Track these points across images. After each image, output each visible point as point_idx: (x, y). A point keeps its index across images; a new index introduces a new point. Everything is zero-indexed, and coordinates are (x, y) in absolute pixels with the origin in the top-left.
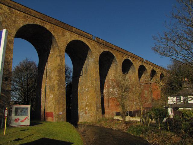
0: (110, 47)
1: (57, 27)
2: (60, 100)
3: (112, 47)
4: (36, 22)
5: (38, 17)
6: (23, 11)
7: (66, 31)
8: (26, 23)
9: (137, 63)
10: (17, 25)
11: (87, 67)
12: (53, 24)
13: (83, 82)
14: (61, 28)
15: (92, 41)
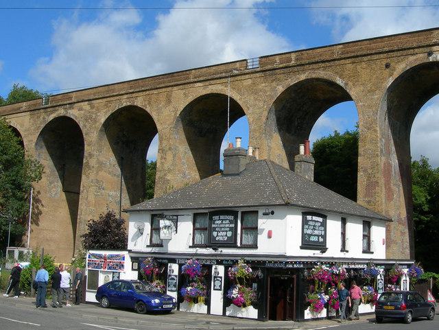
1: (155, 92)
7: (175, 88)
12: (148, 90)
14: (164, 90)
15: (243, 77)
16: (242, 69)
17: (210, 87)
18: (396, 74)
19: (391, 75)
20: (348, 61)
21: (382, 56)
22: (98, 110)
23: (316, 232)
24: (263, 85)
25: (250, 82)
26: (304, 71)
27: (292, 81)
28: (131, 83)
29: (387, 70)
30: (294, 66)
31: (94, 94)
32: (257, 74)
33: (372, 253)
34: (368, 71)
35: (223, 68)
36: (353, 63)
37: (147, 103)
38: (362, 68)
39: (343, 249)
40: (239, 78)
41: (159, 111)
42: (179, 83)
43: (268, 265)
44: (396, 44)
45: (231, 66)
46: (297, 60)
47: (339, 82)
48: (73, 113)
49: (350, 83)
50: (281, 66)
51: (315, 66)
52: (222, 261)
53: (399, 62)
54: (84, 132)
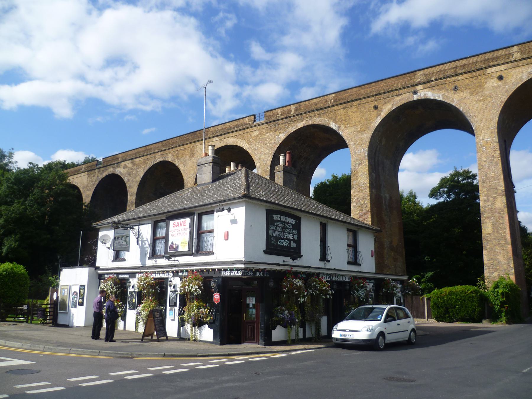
0: (313, 111)
1: (182, 148)
3: (319, 106)
7: (197, 144)
12: (176, 147)
14: (188, 145)
15: (251, 129)
16: (251, 122)
17: (225, 140)
18: (383, 114)
19: (379, 115)
20: (339, 107)
21: (370, 99)
22: (138, 166)
23: (286, 235)
24: (268, 134)
25: (257, 133)
26: (302, 120)
27: (292, 129)
28: (164, 143)
29: (376, 111)
30: (293, 116)
32: (263, 126)
33: (360, 265)
34: (358, 114)
35: (235, 123)
36: (345, 108)
37: (175, 157)
38: (353, 112)
39: (324, 257)
40: (248, 130)
41: (185, 163)
43: (224, 274)
44: (382, 86)
46: (296, 110)
47: (333, 126)
48: (120, 171)
49: (342, 126)
50: (283, 117)
51: (311, 114)
52: (177, 272)
53: (386, 103)
54: (128, 185)
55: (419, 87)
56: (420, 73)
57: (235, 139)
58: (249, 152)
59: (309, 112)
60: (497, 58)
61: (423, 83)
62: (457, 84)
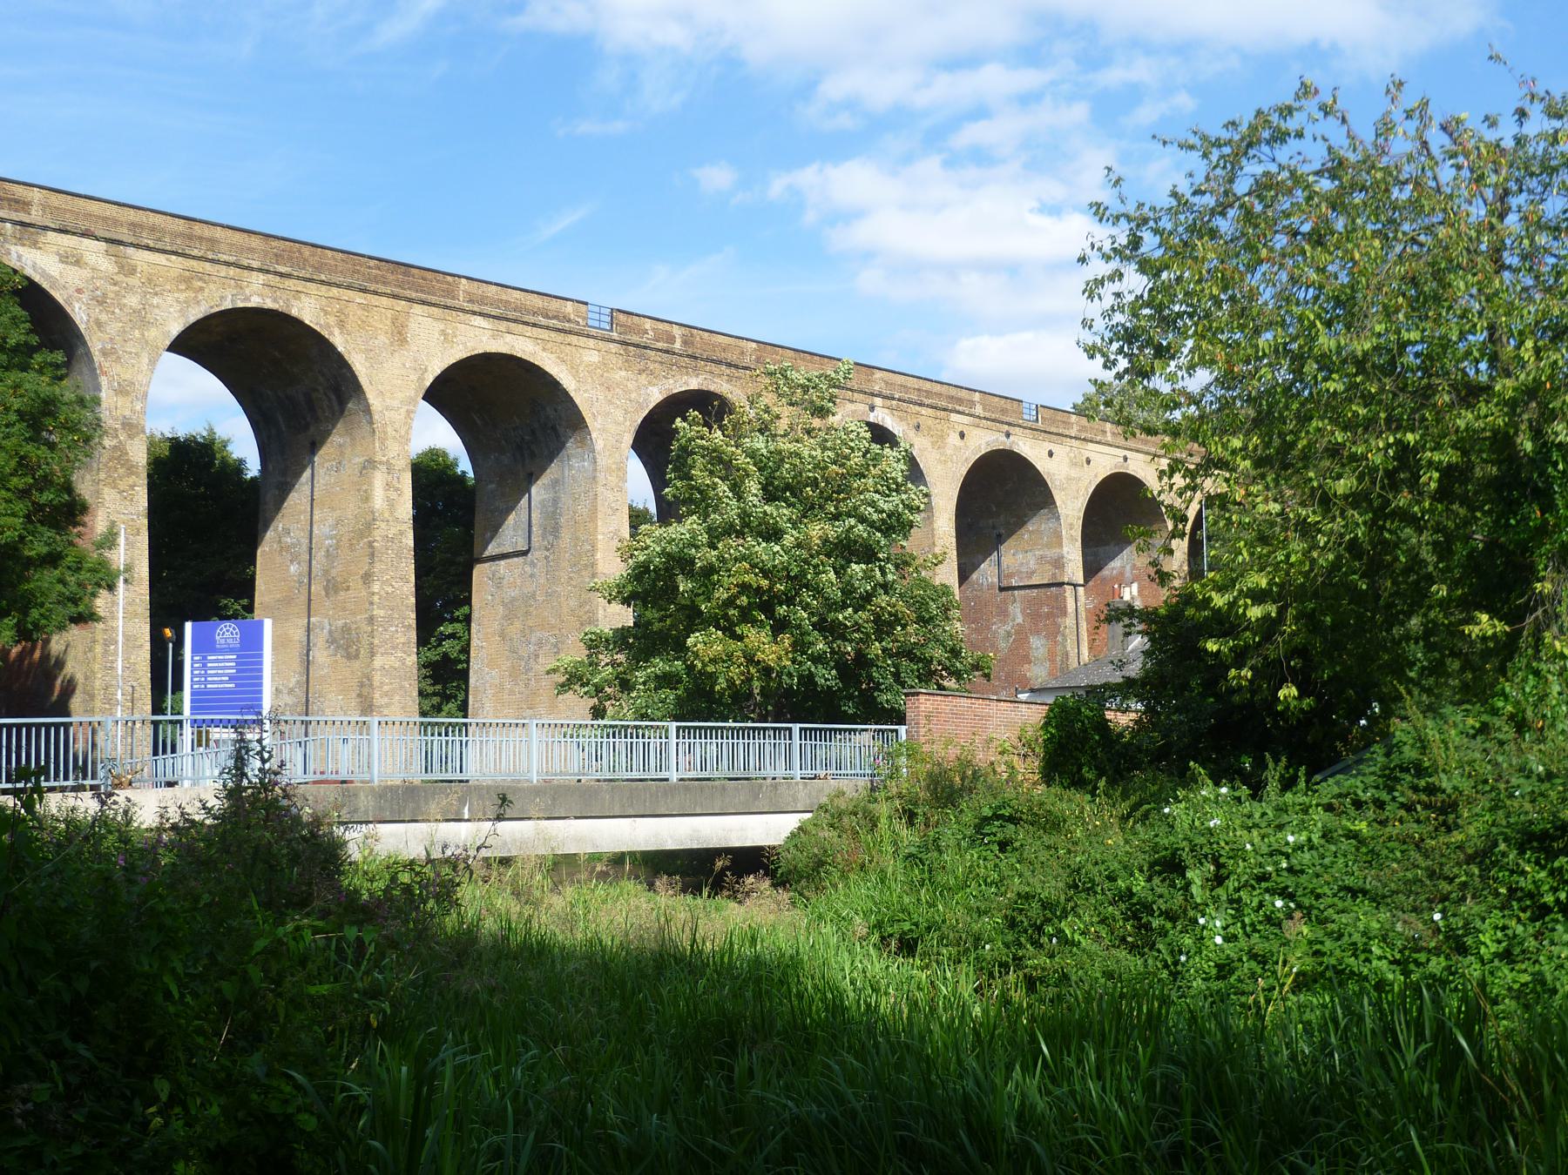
0: (720, 362)
1: (359, 298)
2: (387, 705)
3: (732, 357)
4: (247, 291)
5: (255, 264)
6: (179, 245)
7: (418, 309)
8: (196, 314)
9: (954, 438)
10: (152, 333)
11: (555, 501)
12: (339, 286)
13: (533, 596)
14: (385, 301)
15: (582, 341)
17: (509, 337)
24: (623, 373)
28: (275, 243)
31: (1004, 411)
32: (612, 345)
35: (538, 302)
40: (574, 339)
42: (433, 299)
45: (964, 394)
55: (878, 401)
56: (878, 374)
57: (538, 349)
58: (577, 401)
59: (713, 361)
60: (960, 401)
61: (885, 397)
62: (921, 420)
